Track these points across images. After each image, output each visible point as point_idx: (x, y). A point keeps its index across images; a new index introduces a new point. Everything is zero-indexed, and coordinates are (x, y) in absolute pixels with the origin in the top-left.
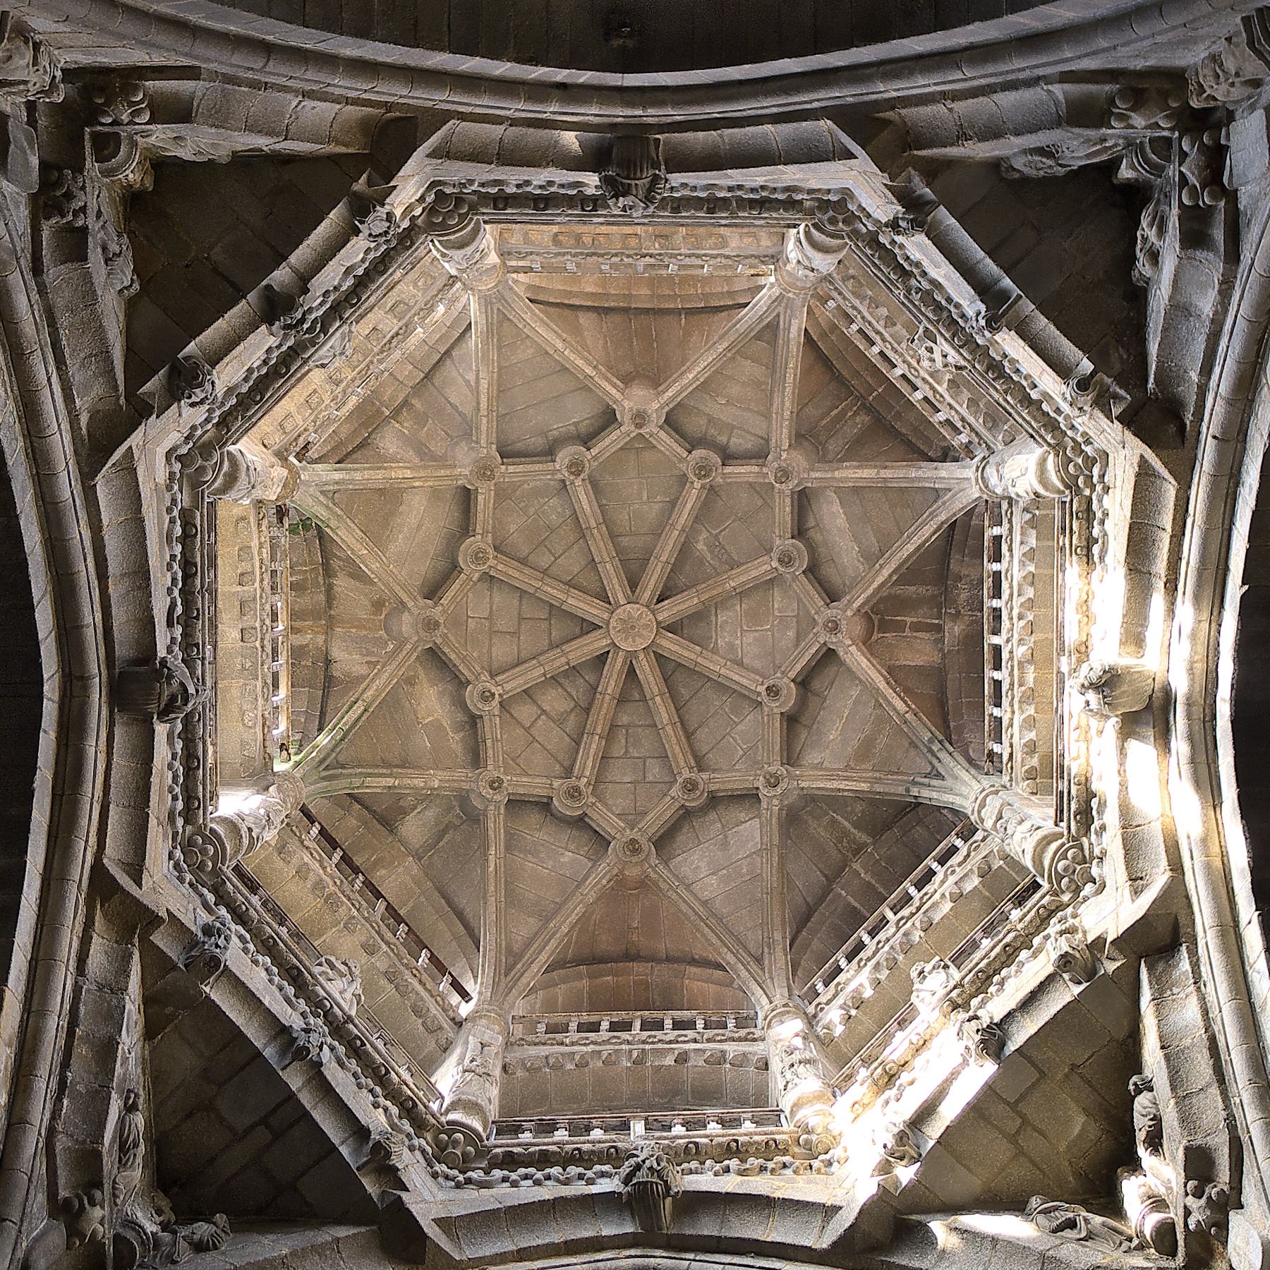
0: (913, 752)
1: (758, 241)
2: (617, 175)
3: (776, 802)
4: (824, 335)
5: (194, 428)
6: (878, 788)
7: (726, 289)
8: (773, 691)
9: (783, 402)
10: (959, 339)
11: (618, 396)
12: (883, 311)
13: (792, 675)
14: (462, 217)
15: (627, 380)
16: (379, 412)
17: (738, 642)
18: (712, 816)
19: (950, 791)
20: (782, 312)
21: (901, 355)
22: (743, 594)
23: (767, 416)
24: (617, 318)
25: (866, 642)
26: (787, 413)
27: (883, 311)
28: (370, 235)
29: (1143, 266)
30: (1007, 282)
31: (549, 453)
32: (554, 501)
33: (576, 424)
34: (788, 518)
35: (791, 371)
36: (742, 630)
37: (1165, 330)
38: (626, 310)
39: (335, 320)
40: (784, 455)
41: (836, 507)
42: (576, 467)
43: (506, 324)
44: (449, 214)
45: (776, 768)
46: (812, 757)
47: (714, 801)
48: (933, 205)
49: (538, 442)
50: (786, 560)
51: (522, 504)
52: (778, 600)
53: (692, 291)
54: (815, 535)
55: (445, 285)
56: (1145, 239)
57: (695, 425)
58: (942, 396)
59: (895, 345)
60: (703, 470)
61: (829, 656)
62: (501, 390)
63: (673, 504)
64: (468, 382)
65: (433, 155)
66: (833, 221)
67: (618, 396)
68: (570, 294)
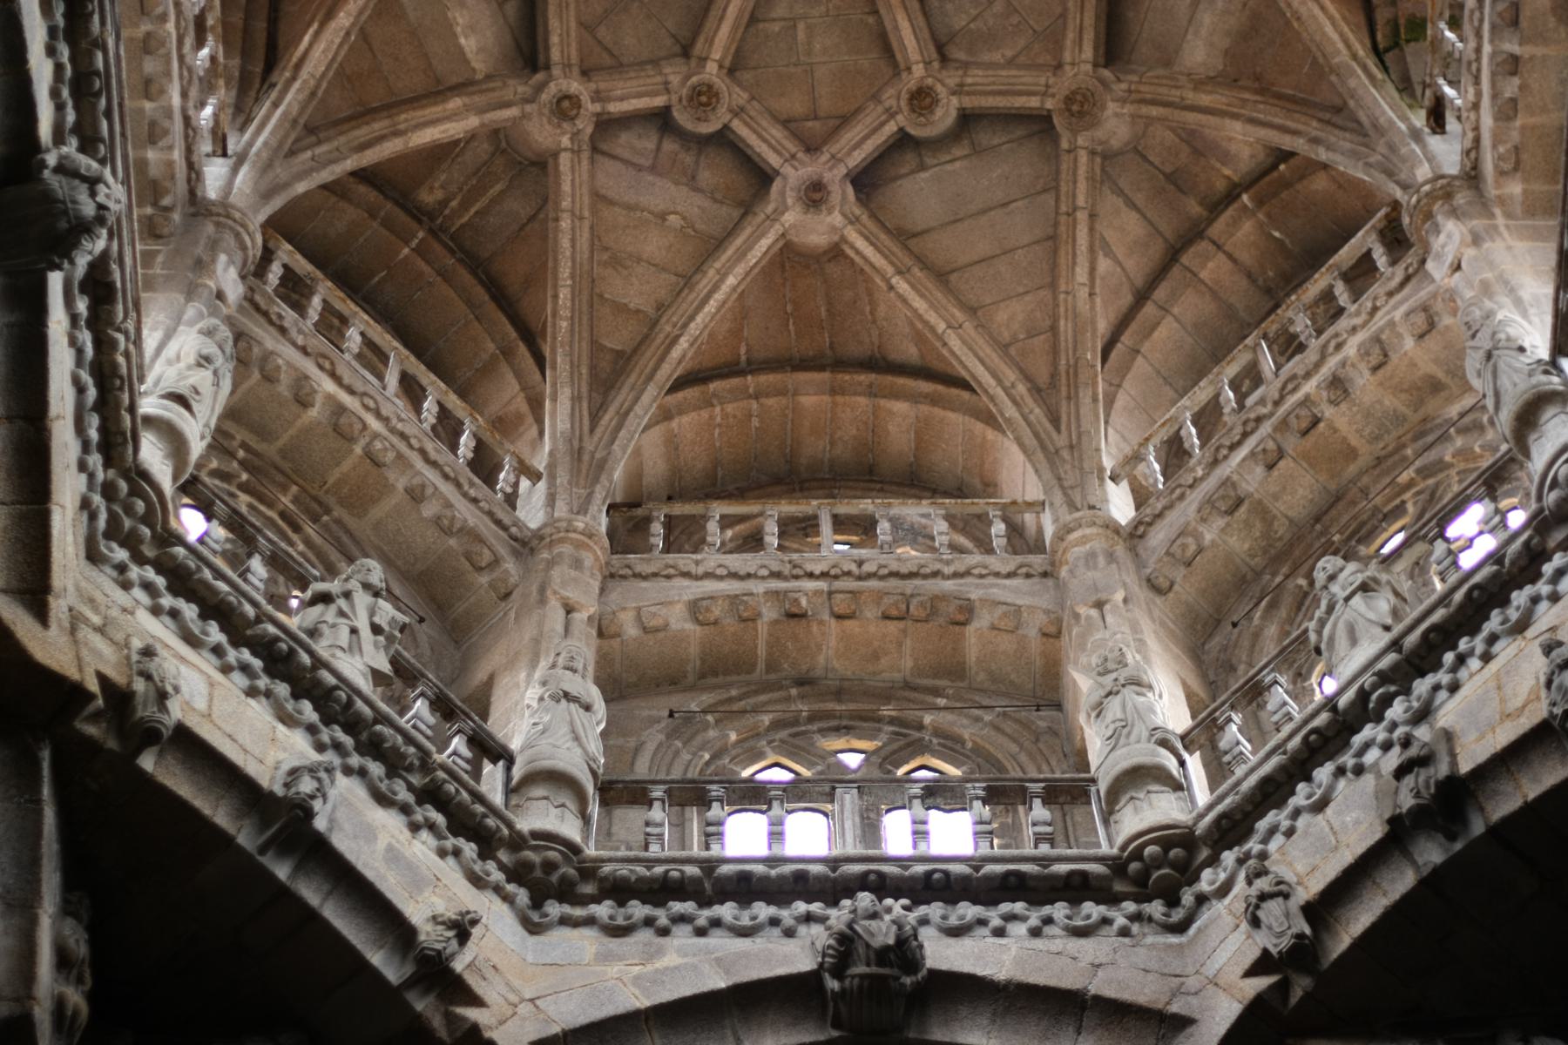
1: (639, 618)
2: (897, 978)
4: (507, 353)
7: (674, 424)
9: (573, 240)
10: (337, 701)
11: (853, 235)
12: (429, 510)
14: (1137, 855)
15: (836, 252)
16: (1260, 202)
20: (586, 438)
21: (393, 430)
23: (599, 198)
24: (854, 350)
26: (565, 224)
27: (429, 510)
28: (1286, 896)
29: (80, 948)
30: (282, 871)
31: (967, 120)
32: (959, 22)
33: (922, 167)
34: (554, 23)
35: (565, 313)
37: (35, 863)
38: (840, 364)
39: (1346, 711)
41: (469, 44)
42: (922, 99)
43: (1043, 378)
44: (1157, 862)
48: (409, 984)
49: (987, 137)
51: (1015, 19)
53: (730, 408)
55: (1150, 524)
56: (80, 981)
57: (715, 172)
58: (321, 368)
59: (402, 447)
60: (703, 98)
62: (1053, 242)
63: (753, 20)
64: (1109, 253)
65: (1183, 1023)
66: (549, 866)
67: (853, 235)
68: (934, 400)
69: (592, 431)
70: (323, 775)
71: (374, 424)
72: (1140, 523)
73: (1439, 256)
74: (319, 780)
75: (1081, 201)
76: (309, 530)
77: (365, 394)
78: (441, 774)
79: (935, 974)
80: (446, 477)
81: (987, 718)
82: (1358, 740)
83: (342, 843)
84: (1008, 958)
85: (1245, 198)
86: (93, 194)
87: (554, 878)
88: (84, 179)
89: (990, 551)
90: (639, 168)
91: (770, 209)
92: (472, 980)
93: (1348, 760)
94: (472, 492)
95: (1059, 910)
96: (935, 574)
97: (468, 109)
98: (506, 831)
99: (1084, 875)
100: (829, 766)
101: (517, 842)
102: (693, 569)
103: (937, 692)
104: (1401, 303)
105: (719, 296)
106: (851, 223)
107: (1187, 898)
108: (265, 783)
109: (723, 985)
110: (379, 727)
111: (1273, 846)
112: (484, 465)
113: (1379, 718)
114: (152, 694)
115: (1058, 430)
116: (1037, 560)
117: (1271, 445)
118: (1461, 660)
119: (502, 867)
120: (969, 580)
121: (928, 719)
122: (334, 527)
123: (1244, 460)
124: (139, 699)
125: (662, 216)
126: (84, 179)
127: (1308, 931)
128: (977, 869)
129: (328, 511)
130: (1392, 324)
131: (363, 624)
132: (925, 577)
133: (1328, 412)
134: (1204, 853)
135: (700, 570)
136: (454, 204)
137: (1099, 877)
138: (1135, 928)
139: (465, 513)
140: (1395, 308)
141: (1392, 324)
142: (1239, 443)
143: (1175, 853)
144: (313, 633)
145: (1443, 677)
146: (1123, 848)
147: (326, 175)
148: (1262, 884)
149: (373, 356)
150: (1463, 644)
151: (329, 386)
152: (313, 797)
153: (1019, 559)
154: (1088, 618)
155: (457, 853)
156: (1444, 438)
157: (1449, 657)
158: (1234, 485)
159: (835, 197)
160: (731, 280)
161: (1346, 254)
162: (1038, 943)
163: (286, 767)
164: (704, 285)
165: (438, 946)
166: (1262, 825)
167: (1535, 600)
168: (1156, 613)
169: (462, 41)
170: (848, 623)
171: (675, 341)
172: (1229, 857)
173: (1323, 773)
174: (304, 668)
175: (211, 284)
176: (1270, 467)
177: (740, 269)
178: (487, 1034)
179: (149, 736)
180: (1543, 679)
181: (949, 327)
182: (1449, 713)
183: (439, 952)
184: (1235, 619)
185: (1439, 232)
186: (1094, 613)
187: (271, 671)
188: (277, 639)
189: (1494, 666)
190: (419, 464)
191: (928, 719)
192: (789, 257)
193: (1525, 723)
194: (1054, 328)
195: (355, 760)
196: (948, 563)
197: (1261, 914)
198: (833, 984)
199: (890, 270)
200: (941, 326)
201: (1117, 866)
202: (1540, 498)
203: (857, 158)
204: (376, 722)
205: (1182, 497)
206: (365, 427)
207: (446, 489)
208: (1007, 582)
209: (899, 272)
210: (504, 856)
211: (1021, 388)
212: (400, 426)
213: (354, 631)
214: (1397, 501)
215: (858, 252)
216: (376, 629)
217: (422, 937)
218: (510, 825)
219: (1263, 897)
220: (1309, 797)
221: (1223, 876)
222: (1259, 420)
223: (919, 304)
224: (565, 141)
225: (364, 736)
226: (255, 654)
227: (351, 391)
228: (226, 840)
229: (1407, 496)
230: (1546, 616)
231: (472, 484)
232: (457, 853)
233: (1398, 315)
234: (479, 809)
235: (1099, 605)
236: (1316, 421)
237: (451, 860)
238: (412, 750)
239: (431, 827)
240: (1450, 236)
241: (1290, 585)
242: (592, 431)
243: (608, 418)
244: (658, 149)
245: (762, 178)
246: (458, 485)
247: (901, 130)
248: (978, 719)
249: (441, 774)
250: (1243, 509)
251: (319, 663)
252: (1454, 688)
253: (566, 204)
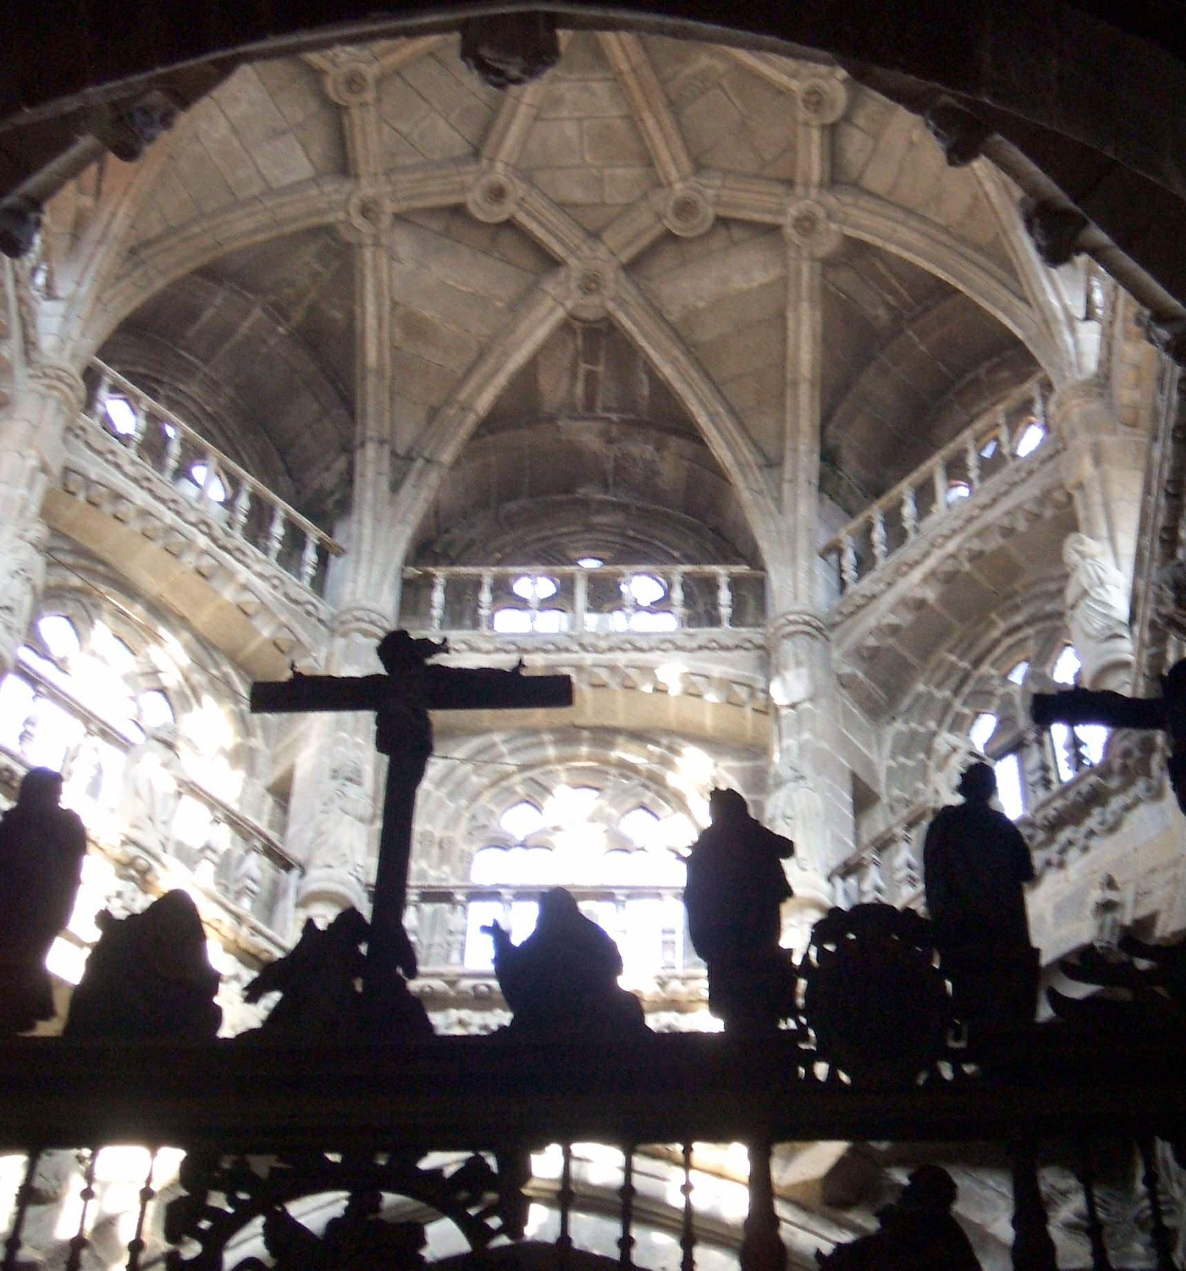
0: (421, 414)
3: (341, 216)
6: (371, 383)
8: (497, 194)
12: (1021, 525)
13: (522, 218)
17: (565, 113)
18: (313, 105)
19: (377, 520)
21: (962, 528)
22: (633, 120)
25: (566, 327)
27: (1021, 525)
36: (580, 120)
40: (834, 227)
41: (760, 277)
45: (389, 207)
46: (404, 243)
47: (336, 113)
50: (685, 208)
52: (625, 174)
54: (716, 243)
61: (551, 263)
71: (951, 546)
87: (1137, 754)
90: (874, 150)
97: (796, 309)
125: (912, 144)
136: (890, 298)
151: (917, 575)
169: (755, 284)
227: (926, 555)
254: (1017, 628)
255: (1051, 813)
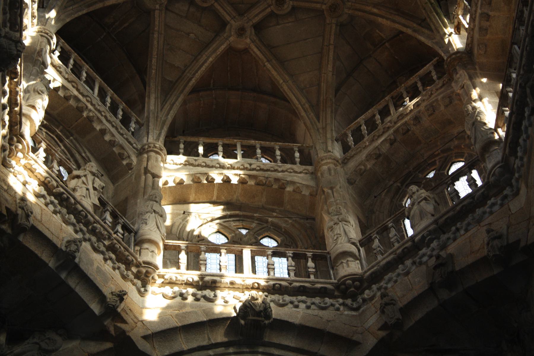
2: (263, 321)
5: (502, 205)
9: (158, 42)
10: (82, 215)
11: (253, 47)
12: (107, 138)
20: (159, 113)
21: (96, 109)
26: (156, 36)
27: (107, 138)
33: (278, 24)
55: (349, 159)
58: (73, 87)
59: (99, 115)
65: (357, 344)
67: (253, 47)
69: (161, 110)
70: (78, 243)
71: (90, 106)
72: (346, 158)
73: (456, 82)
74: (77, 245)
75: (332, 42)
76: (67, 141)
77: (87, 96)
78: (115, 241)
79: (275, 320)
80: (113, 126)
81: (290, 221)
82: (421, 252)
83: (83, 266)
84: (299, 316)
85: (387, 44)
86: (16, 47)
88: (13, 41)
89: (294, 163)
91: (225, 35)
92: (123, 315)
93: (417, 259)
94: (121, 131)
95: (317, 300)
96: (276, 171)
98: (135, 261)
99: (325, 288)
100: (236, 235)
101: (138, 265)
102: (194, 162)
103: (273, 211)
104: (441, 93)
105: (206, 65)
106: (253, 42)
107: (360, 300)
108: (59, 246)
109: (205, 320)
110: (95, 225)
111: (389, 285)
112: (125, 121)
113: (428, 246)
114: (24, 215)
115: (319, 122)
116: (309, 168)
117: (392, 137)
118: (458, 230)
119: (133, 273)
120: (286, 173)
121: (270, 219)
122: (74, 141)
123: (383, 141)
124: (19, 217)
125: (188, 34)
126: (13, 41)
127: (401, 318)
128: (290, 284)
129: (72, 135)
130: (437, 100)
131: (90, 187)
132: (272, 171)
133: (413, 128)
134: (366, 284)
135: (197, 163)
137: (330, 290)
138: (342, 308)
139: (119, 139)
140: (439, 95)
141: (437, 100)
142: (382, 135)
143: (357, 283)
144: (74, 190)
145: (450, 235)
146: (339, 281)
147: (76, 16)
148: (386, 299)
149: (90, 82)
150: (458, 225)
152: (75, 252)
153: (304, 167)
154: (328, 193)
155: (119, 268)
156: (452, 140)
157: (454, 228)
158: (379, 149)
159: (248, 33)
160: (211, 59)
161: (422, 72)
162: (309, 311)
163: (66, 240)
164: (201, 61)
165: (113, 304)
166: (386, 277)
167: (484, 213)
168: (350, 191)
170: (245, 185)
171: (190, 79)
172: (374, 287)
173: (408, 262)
174: (72, 204)
175: (40, 59)
176: (391, 144)
177: (214, 56)
178: (128, 334)
179: (23, 229)
180: (486, 242)
181: (284, 82)
182: (452, 248)
183: (114, 306)
184: (376, 195)
185: (457, 73)
186: (330, 191)
187: (61, 204)
188: (63, 193)
189: (469, 234)
190: (104, 121)
191: (270, 219)
192: (231, 50)
193: (479, 256)
194: (319, 85)
195: (87, 236)
196: (280, 167)
197: (385, 310)
198: (242, 322)
199: (265, 60)
200: (281, 81)
201: (337, 286)
202: (488, 178)
203: (256, 20)
204: (94, 223)
205: (361, 151)
206: (87, 107)
207: (113, 130)
208: (299, 175)
209: (268, 61)
210: (134, 270)
211: (307, 106)
212: (98, 108)
213: (87, 189)
214: (433, 160)
215: (254, 52)
216: (95, 189)
217: (108, 300)
218: (136, 259)
219: (387, 304)
220: (403, 270)
221: (372, 294)
222: (389, 128)
223: (274, 73)
224: (157, 6)
225: (90, 227)
226: (55, 198)
227: (83, 96)
228: (45, 265)
229: (437, 158)
230: (488, 219)
231: (121, 128)
232: (119, 268)
233: (439, 98)
234: (127, 253)
235: (332, 188)
236: (408, 130)
237: (117, 271)
238: (106, 233)
239: (111, 259)
240: (462, 75)
241: (395, 185)
242: (161, 110)
243: (167, 106)
244: (188, 10)
245: (224, 24)
246: (117, 129)
247: (272, 11)
248: (286, 221)
249: (115, 241)
250: (381, 158)
251: (77, 202)
252: (455, 239)
253: (156, 28)
254: (61, 141)
255: (118, 246)
